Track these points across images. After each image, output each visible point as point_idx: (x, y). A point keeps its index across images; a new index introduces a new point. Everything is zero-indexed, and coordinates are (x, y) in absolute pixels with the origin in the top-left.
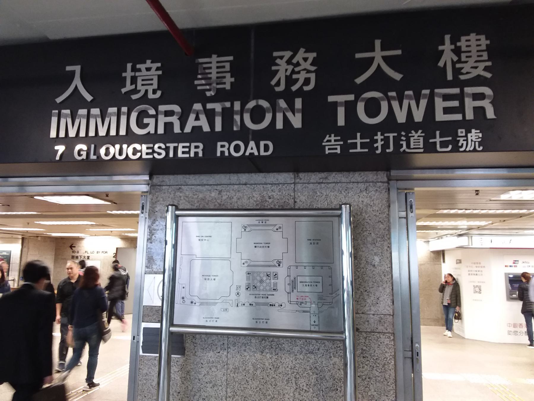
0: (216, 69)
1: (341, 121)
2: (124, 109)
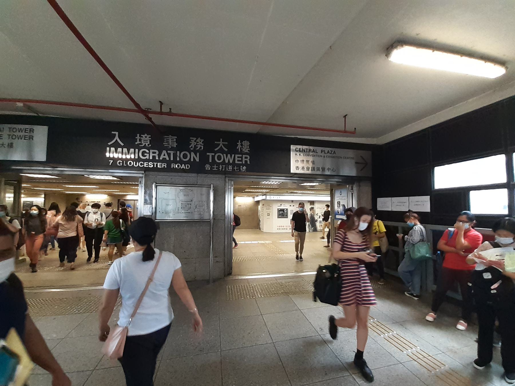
0: (171, 141)
1: (210, 161)
2: (137, 150)
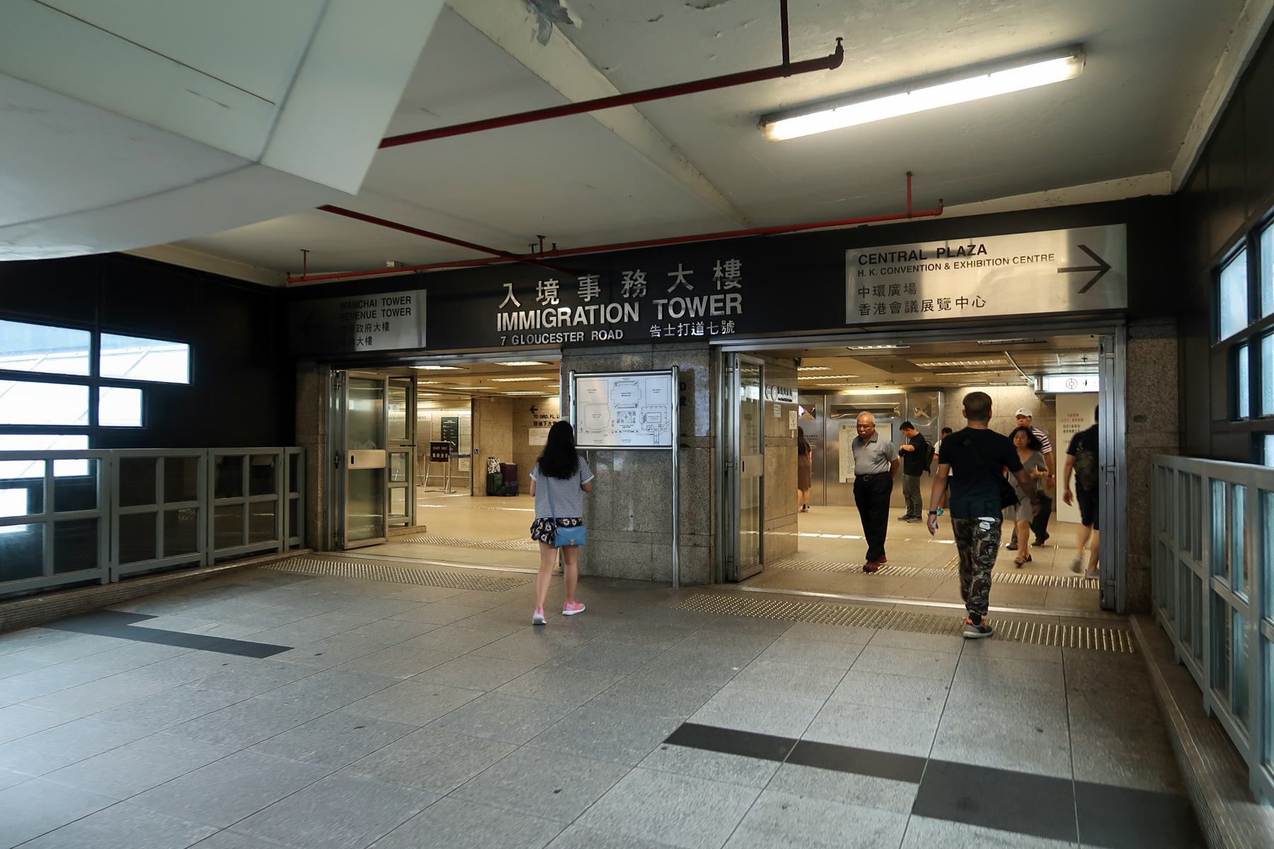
0: (589, 287)
1: (660, 317)
